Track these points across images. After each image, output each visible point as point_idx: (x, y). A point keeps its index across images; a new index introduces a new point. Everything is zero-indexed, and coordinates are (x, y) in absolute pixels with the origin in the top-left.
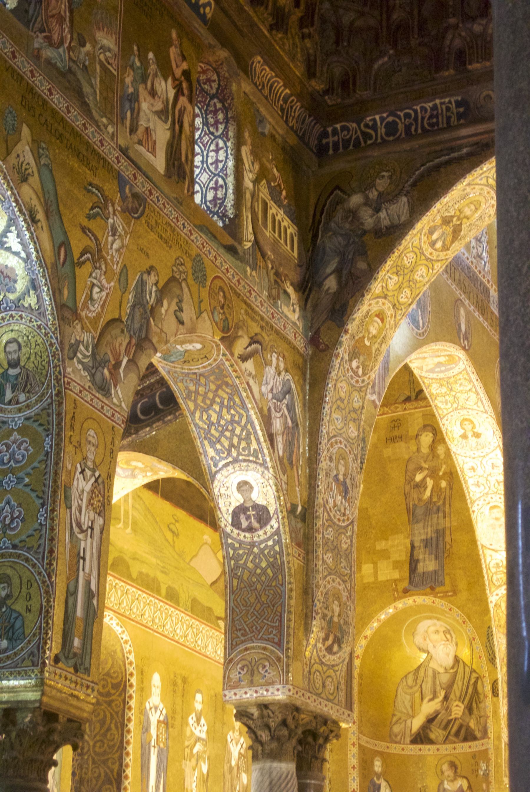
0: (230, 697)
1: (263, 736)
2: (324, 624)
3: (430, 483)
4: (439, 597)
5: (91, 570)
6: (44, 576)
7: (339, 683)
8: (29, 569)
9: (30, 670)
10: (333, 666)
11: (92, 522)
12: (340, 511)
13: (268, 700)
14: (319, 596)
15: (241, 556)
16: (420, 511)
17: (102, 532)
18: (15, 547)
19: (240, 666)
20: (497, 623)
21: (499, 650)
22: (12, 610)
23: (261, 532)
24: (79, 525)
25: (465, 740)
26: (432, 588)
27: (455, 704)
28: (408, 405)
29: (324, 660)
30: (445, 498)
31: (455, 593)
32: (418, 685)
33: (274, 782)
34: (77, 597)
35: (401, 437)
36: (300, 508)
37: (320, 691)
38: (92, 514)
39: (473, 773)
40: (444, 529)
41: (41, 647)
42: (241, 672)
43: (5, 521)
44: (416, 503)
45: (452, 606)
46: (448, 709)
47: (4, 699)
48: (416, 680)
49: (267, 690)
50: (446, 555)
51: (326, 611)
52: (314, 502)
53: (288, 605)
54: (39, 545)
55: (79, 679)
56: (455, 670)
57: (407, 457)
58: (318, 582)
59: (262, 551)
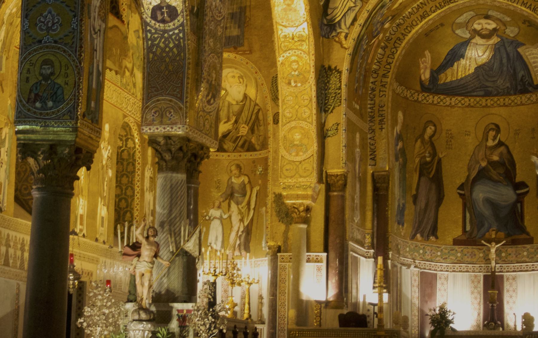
0: (146, 131)
1: (167, 156)
2: (208, 86)
5: (99, 59)
6: (77, 63)
7: (212, 123)
8: (66, 57)
9: (68, 121)
10: (210, 112)
11: (100, 26)
12: (218, 10)
13: (172, 134)
14: (206, 68)
15: (155, 39)
17: (104, 33)
18: (55, 42)
19: (153, 111)
20: (282, 75)
21: (281, 94)
22: (55, 83)
23: (171, 24)
24: (94, 29)
25: (248, 150)
26: (235, 48)
29: (205, 109)
31: (251, 52)
33: (173, 186)
34: (93, 75)
36: (196, 9)
37: (202, 129)
38: (100, 21)
39: (252, 173)
40: (245, 7)
41: (75, 107)
42: (154, 115)
43: (48, 24)
45: (248, 61)
47: (50, 139)
49: (172, 128)
50: (246, 25)
51: (209, 78)
52: (204, 4)
53: (187, 73)
54: (73, 43)
55: (93, 127)
56: (244, 103)
58: (205, 58)
59: (170, 36)
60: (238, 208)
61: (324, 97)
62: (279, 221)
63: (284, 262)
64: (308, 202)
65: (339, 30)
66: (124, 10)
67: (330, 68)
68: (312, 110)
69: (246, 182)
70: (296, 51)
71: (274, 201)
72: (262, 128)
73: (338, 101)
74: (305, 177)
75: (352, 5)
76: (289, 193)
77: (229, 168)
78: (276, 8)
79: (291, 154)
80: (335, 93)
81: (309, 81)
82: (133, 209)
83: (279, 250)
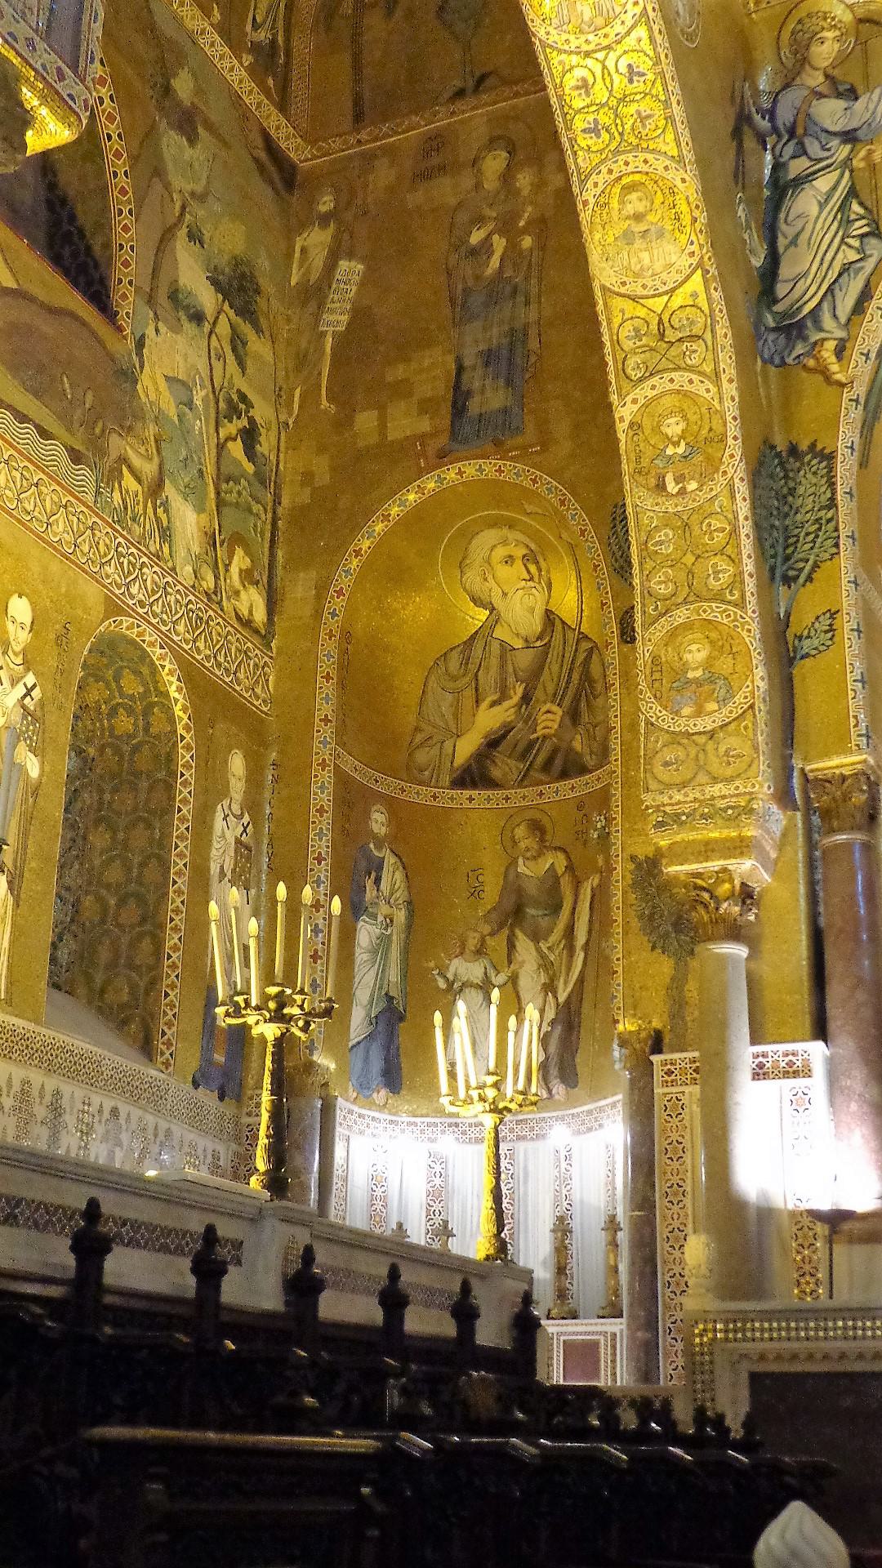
3: (499, 243)
4: (512, 459)
16: (477, 301)
25: (564, 775)
26: (498, 443)
27: (544, 709)
28: (459, 105)
30: (530, 265)
31: (546, 442)
32: (470, 675)
35: (442, 169)
40: (526, 327)
44: (470, 283)
46: (530, 721)
48: (466, 661)
57: (453, 201)
60: (539, 950)
61: (781, 540)
62: (653, 948)
63: (673, 1083)
64: (744, 867)
65: (815, 336)
66: (124, 297)
67: (793, 450)
68: (741, 561)
69: (560, 870)
70: (673, 375)
71: (635, 885)
72: (600, 701)
73: (830, 542)
74: (728, 780)
75: (853, 256)
76: (678, 838)
77: (508, 833)
78: (597, 236)
79: (677, 713)
80: (817, 520)
81: (722, 468)
82: (161, 927)
83: (657, 1048)
